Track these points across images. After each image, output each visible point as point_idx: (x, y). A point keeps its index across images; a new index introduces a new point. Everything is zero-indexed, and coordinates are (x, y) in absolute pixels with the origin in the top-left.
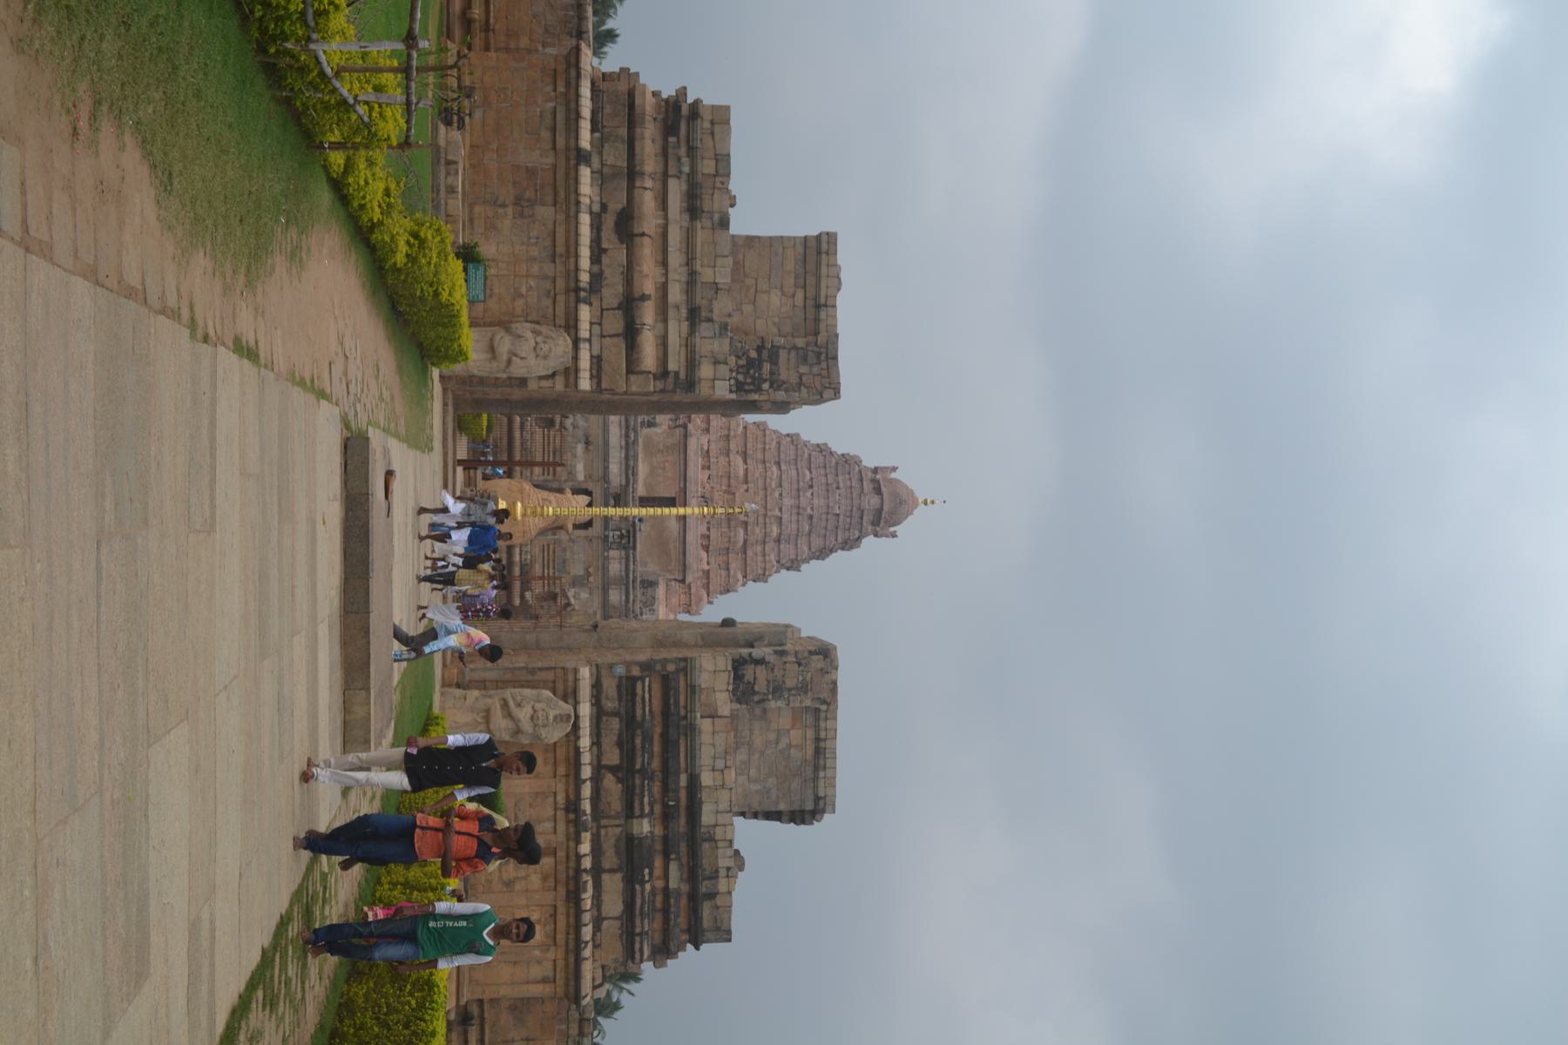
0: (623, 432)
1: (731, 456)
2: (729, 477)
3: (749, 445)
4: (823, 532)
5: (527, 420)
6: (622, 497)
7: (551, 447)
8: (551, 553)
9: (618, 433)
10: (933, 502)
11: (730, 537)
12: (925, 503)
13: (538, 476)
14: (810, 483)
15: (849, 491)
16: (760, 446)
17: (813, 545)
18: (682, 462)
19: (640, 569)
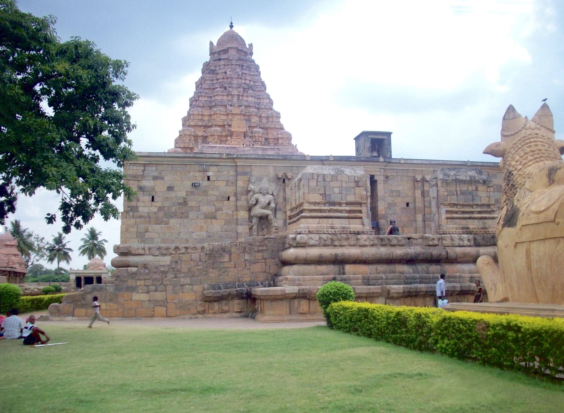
2: (221, 136)
3: (200, 124)
4: (252, 83)
5: (295, 239)
7: (323, 208)
8: (455, 209)
11: (259, 136)
12: (231, 27)
13: (363, 224)
14: (223, 89)
15: (226, 67)
17: (261, 89)
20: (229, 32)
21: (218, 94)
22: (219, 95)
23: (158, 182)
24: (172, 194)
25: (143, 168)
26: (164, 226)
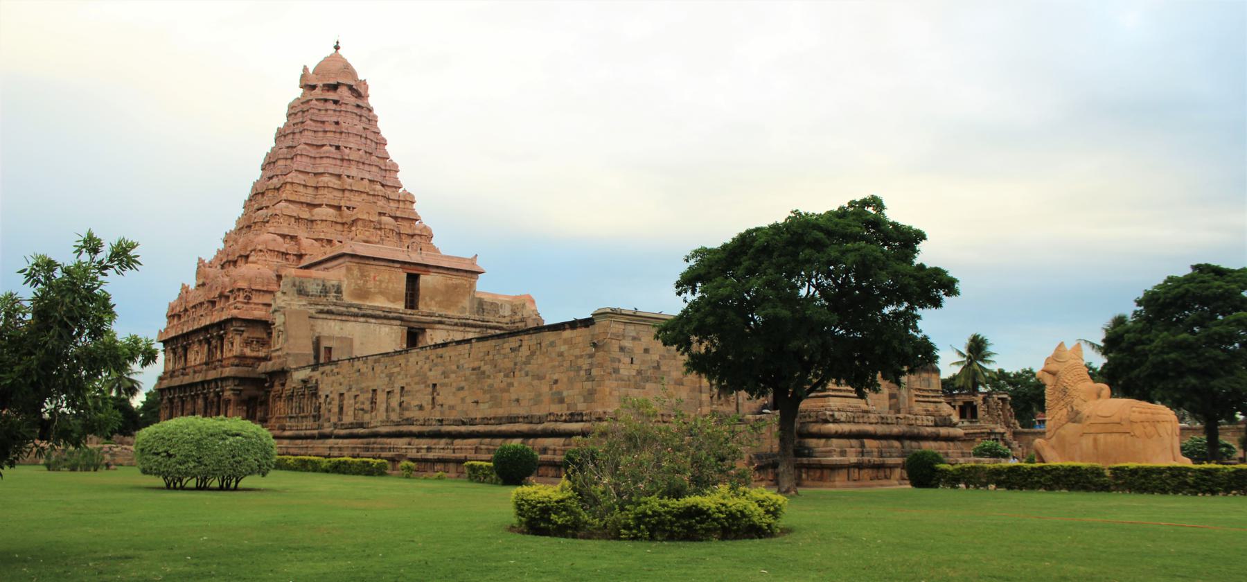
0: (352, 319)
1: (313, 218)
2: (336, 223)
3: (303, 199)
6: (412, 325)
9: (349, 324)
10: (338, 42)
11: (390, 229)
12: (337, 48)
16: (301, 189)
18: (376, 263)
19: (467, 315)
20: (331, 56)
21: (328, 155)
22: (329, 157)
23: (637, 342)
24: (648, 357)
25: (623, 328)
26: (641, 391)
